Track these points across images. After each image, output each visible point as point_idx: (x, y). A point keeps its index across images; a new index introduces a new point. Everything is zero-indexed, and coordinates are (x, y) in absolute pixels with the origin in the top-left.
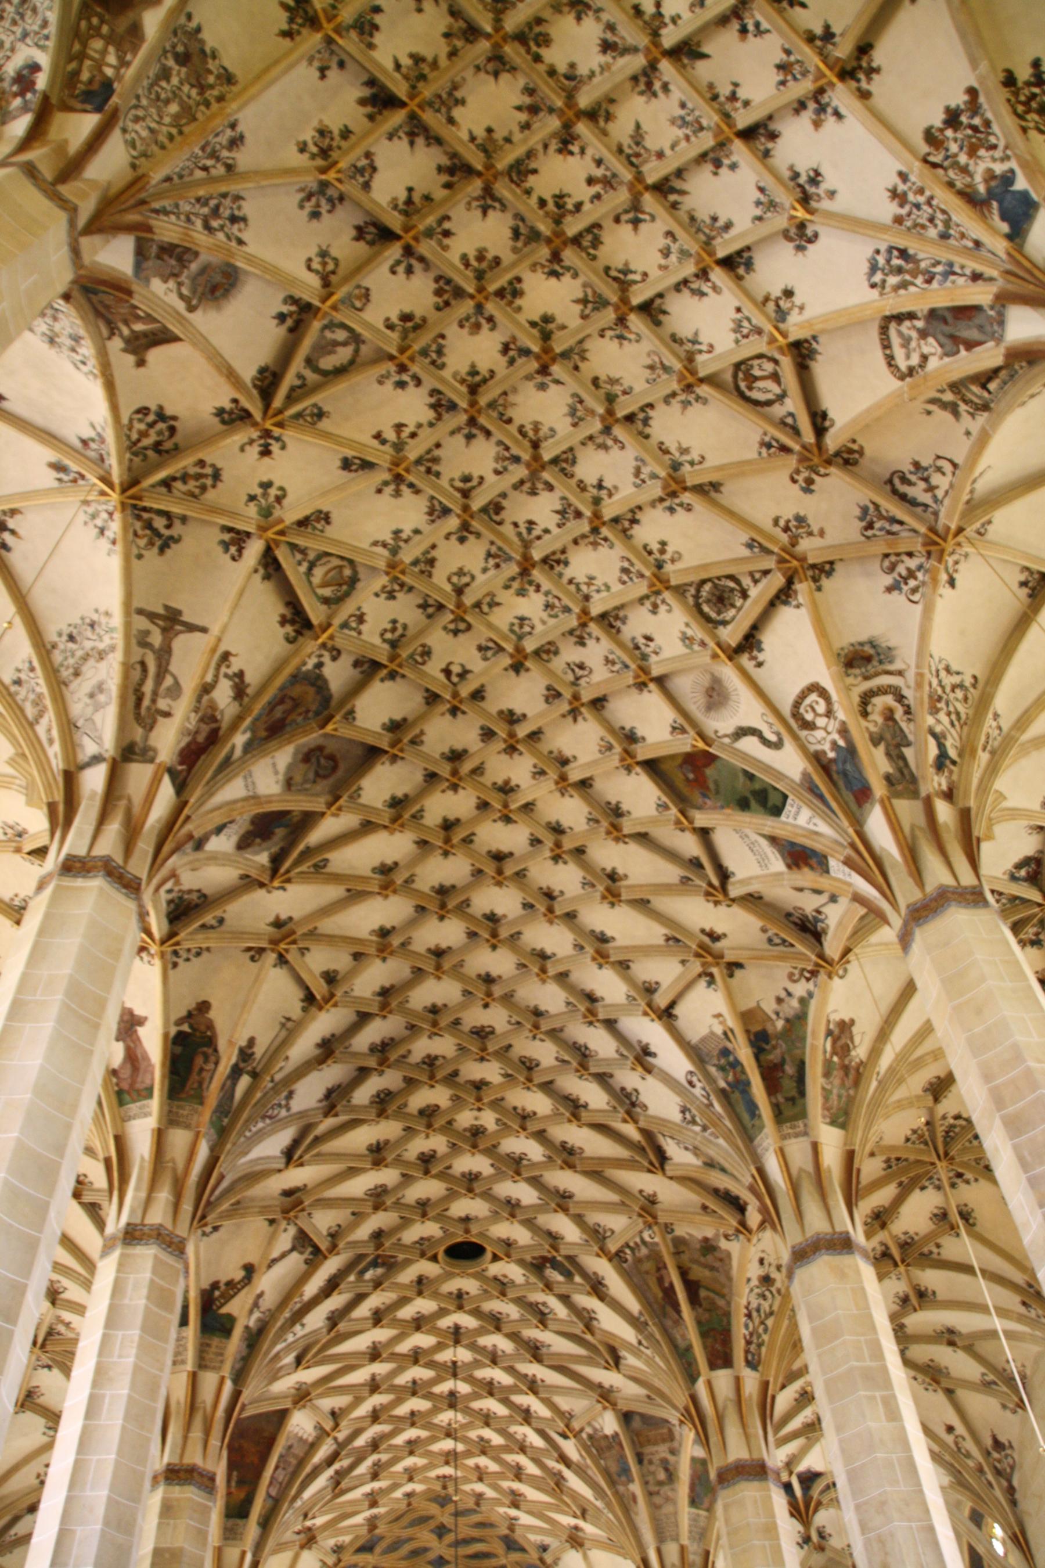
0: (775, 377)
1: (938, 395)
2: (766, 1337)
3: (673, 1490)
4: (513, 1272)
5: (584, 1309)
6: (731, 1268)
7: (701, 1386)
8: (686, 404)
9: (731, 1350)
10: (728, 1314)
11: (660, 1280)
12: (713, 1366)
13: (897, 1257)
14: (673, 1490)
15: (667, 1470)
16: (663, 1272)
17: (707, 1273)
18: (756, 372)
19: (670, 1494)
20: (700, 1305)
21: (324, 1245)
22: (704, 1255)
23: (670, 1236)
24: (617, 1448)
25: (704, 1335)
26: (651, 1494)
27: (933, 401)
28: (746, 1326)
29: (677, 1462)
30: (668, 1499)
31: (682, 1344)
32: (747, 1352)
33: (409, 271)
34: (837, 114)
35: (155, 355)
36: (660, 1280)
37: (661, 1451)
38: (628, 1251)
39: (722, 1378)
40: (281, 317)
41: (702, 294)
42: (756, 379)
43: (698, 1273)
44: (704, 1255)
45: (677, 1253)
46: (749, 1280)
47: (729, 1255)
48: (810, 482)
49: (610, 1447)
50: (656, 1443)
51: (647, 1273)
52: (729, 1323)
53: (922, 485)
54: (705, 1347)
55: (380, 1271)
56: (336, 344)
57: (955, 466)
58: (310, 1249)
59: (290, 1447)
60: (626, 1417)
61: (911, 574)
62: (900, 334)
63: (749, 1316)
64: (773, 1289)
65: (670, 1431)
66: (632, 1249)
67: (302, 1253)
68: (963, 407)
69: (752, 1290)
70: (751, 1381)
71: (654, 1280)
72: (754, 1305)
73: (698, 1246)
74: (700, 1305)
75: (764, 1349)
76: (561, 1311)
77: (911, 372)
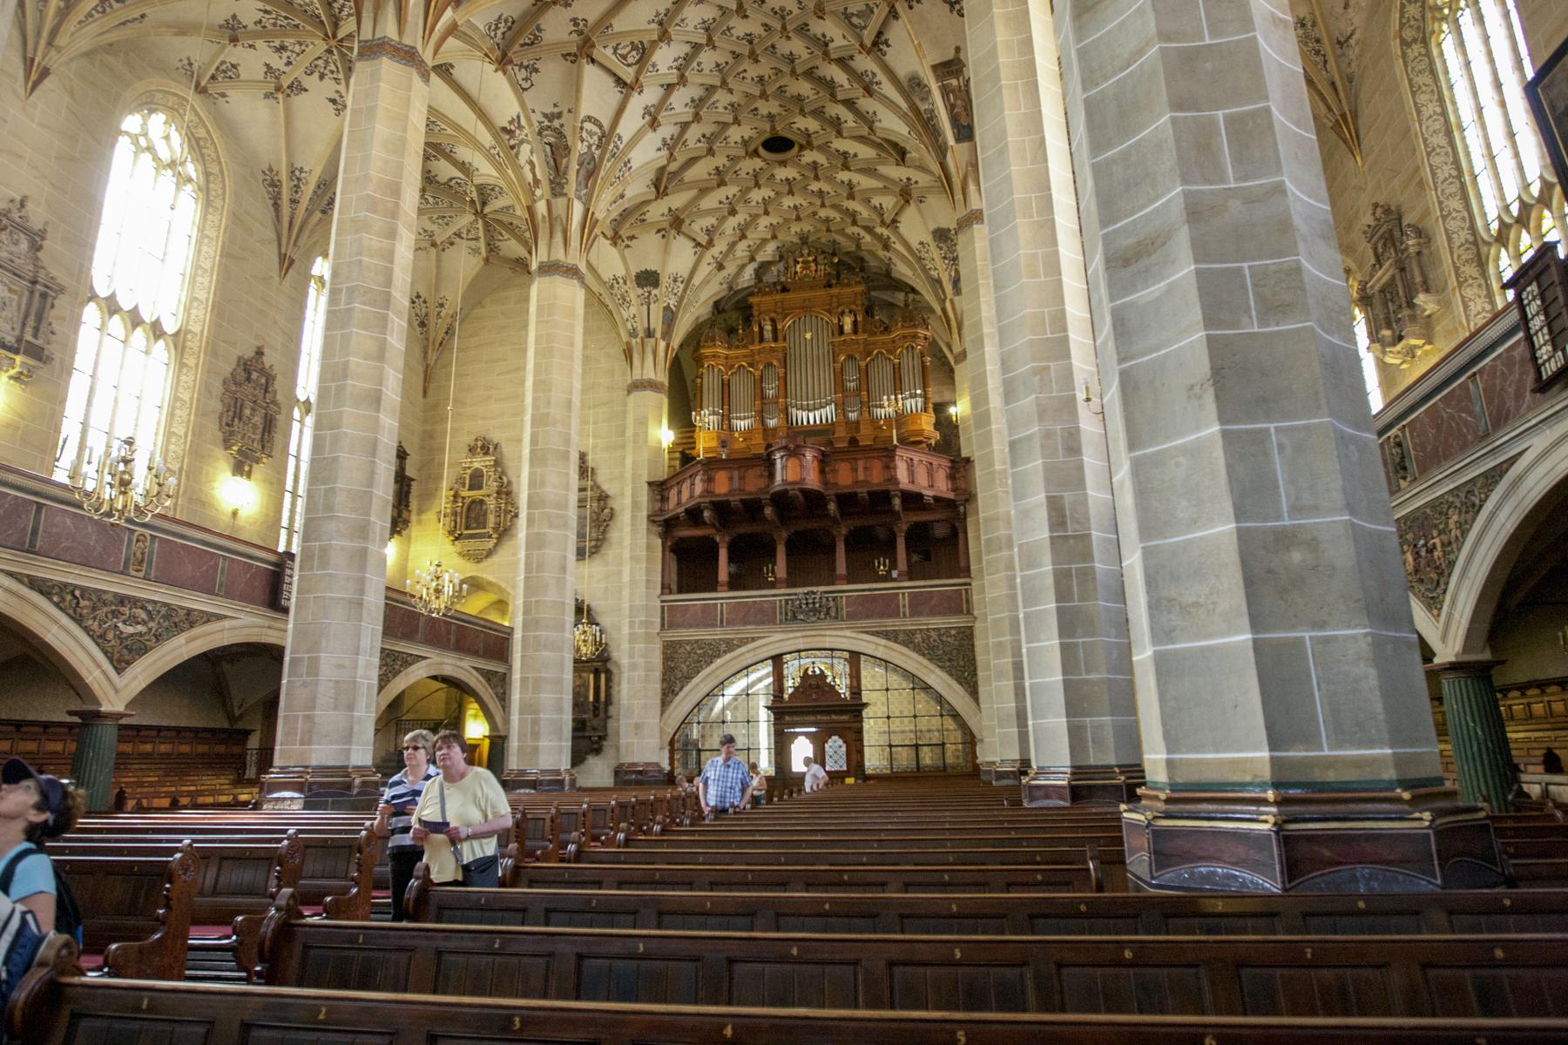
0: (624, 57)
1: (561, 121)
8: (658, 14)
18: (634, 53)
27: (559, 115)
33: (824, 36)
34: (659, 149)
35: (951, 55)
40: (886, 43)
41: (676, 60)
42: (632, 50)
48: (576, 24)
53: (526, 63)
56: (857, 16)
57: (524, 89)
61: (497, 28)
62: (595, 133)
68: (547, 123)
77: (582, 128)
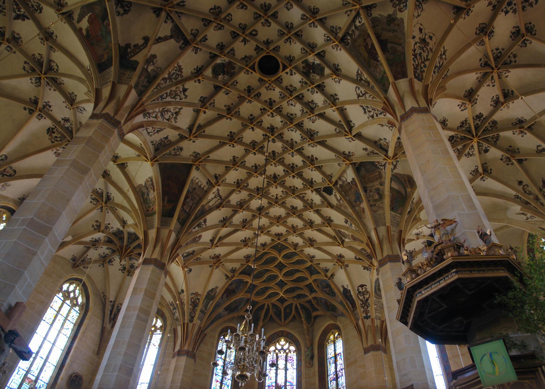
2: (425, 69)
3: (382, 203)
4: (296, 79)
5: (331, 95)
6: (404, 28)
7: (391, 90)
9: (406, 70)
10: (403, 54)
11: (366, 46)
12: (396, 78)
13: (494, 66)
14: (382, 203)
15: (379, 194)
16: (368, 40)
17: (391, 34)
19: (381, 205)
20: (388, 52)
21: (189, 37)
22: (389, 25)
23: (370, 18)
24: (354, 187)
25: (390, 65)
26: (371, 206)
28: (414, 61)
29: (384, 189)
30: (380, 208)
31: (379, 76)
32: (415, 73)
36: (366, 46)
37: (376, 184)
38: (349, 38)
39: (403, 84)
43: (386, 35)
44: (389, 25)
45: (374, 27)
46: (414, 37)
47: (402, 20)
49: (350, 189)
50: (373, 181)
51: (359, 46)
52: (404, 58)
54: (391, 70)
55: (226, 77)
58: (182, 41)
59: (194, 189)
60: (358, 168)
63: (415, 55)
64: (428, 48)
65: (380, 173)
66: (351, 35)
67: (178, 42)
69: (416, 43)
70: (418, 86)
71: (364, 48)
72: (418, 51)
73: (385, 21)
74: (388, 52)
75: (424, 74)
76: (318, 98)
